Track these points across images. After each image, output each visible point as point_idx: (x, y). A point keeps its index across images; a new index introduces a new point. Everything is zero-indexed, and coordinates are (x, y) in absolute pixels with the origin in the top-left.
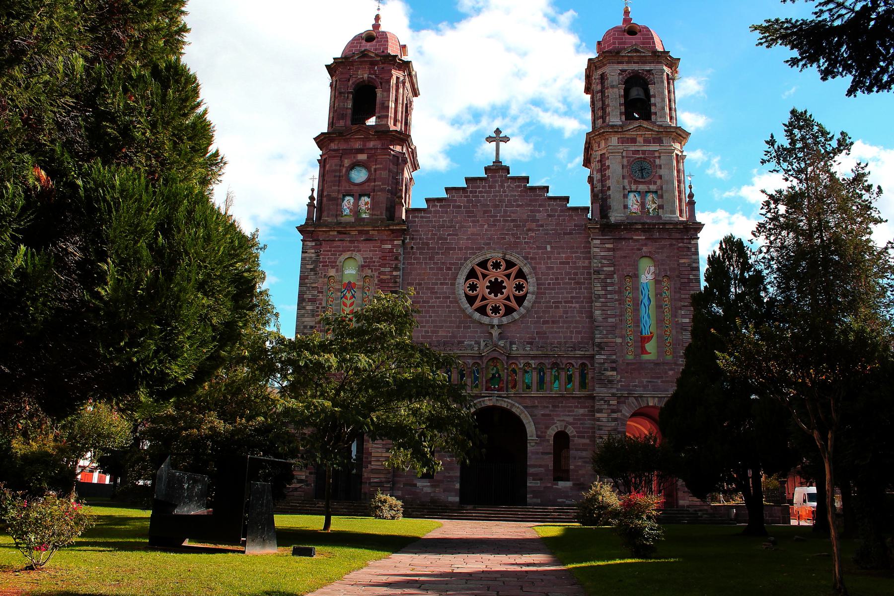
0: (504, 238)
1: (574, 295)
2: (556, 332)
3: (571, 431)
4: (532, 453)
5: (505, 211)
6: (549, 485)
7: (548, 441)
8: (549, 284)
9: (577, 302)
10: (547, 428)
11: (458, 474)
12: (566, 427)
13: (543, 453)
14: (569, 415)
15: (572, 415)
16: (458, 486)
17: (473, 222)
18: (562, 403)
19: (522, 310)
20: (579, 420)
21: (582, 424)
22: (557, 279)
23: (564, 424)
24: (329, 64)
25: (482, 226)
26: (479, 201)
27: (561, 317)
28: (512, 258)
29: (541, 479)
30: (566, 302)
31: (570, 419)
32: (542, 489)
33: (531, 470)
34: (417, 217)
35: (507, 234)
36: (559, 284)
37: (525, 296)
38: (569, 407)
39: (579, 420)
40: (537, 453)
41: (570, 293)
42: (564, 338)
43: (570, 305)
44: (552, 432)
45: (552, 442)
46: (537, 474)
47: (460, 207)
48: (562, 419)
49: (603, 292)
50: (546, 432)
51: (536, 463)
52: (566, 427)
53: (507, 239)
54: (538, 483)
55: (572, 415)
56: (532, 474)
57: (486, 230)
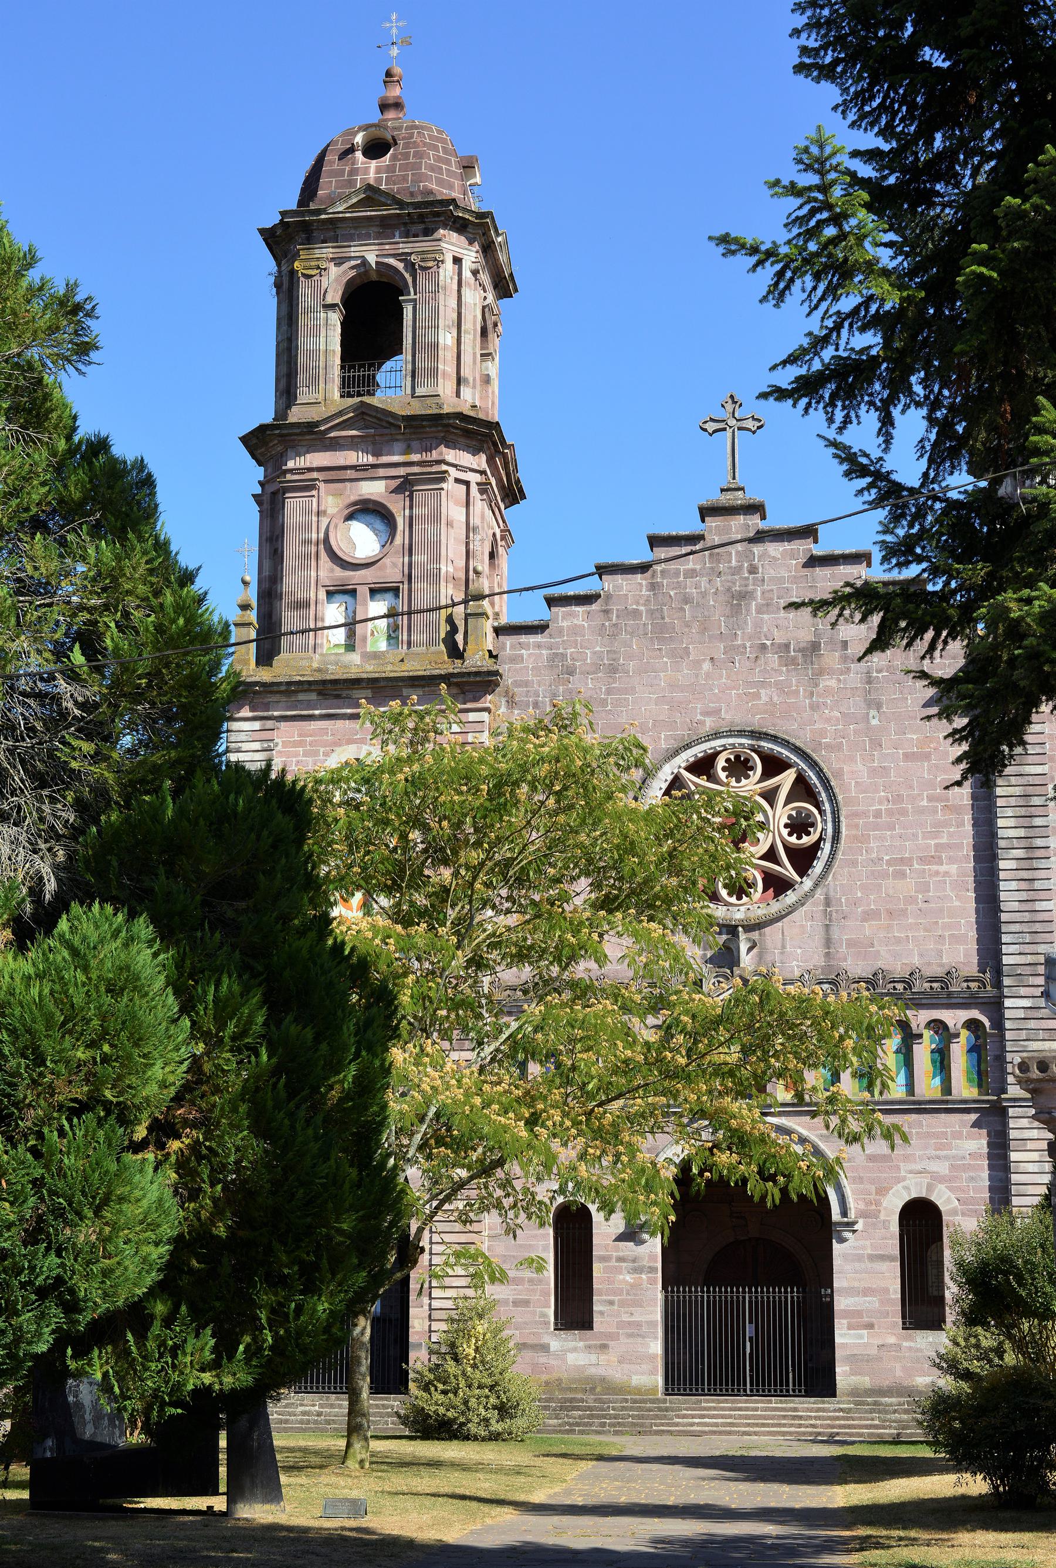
0: (757, 696)
1: (944, 841)
2: (898, 941)
3: (943, 1199)
4: (845, 1257)
5: (758, 625)
6: (892, 1340)
7: (886, 1224)
8: (878, 814)
9: (951, 860)
10: (882, 1191)
11: (657, 1314)
12: (930, 1188)
13: (872, 1258)
14: (938, 1158)
15: (946, 1158)
16: (657, 1347)
17: (673, 654)
18: (921, 1125)
19: (808, 883)
20: (966, 1168)
21: (972, 1179)
22: (899, 799)
23: (926, 1180)
24: (269, 225)
25: (698, 663)
26: (687, 600)
27: (912, 900)
28: (777, 749)
29: (870, 1326)
30: (922, 860)
31: (942, 1168)
32: (874, 1351)
33: (841, 1303)
34: (527, 646)
35: (763, 684)
36: (904, 812)
37: (816, 847)
38: (936, 1135)
39: (966, 1168)
40: (859, 1258)
41: (936, 835)
42: (921, 955)
43: (935, 867)
44: (895, 1202)
45: (895, 1228)
46: (859, 1313)
47: (636, 614)
48: (918, 1167)
49: (1022, 833)
50: (878, 1203)
51: (856, 1284)
52: (930, 1188)
53: (764, 698)
54: (861, 1337)
55: (946, 1158)
56: (848, 1314)
57: (708, 675)
